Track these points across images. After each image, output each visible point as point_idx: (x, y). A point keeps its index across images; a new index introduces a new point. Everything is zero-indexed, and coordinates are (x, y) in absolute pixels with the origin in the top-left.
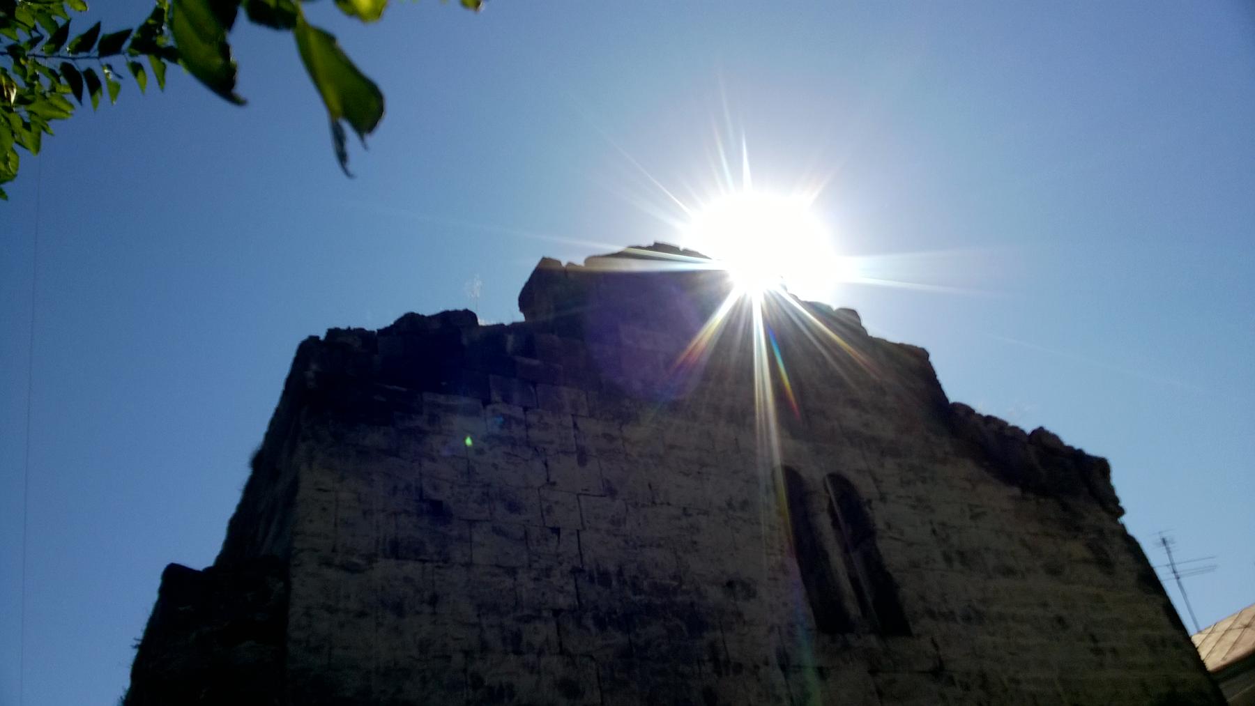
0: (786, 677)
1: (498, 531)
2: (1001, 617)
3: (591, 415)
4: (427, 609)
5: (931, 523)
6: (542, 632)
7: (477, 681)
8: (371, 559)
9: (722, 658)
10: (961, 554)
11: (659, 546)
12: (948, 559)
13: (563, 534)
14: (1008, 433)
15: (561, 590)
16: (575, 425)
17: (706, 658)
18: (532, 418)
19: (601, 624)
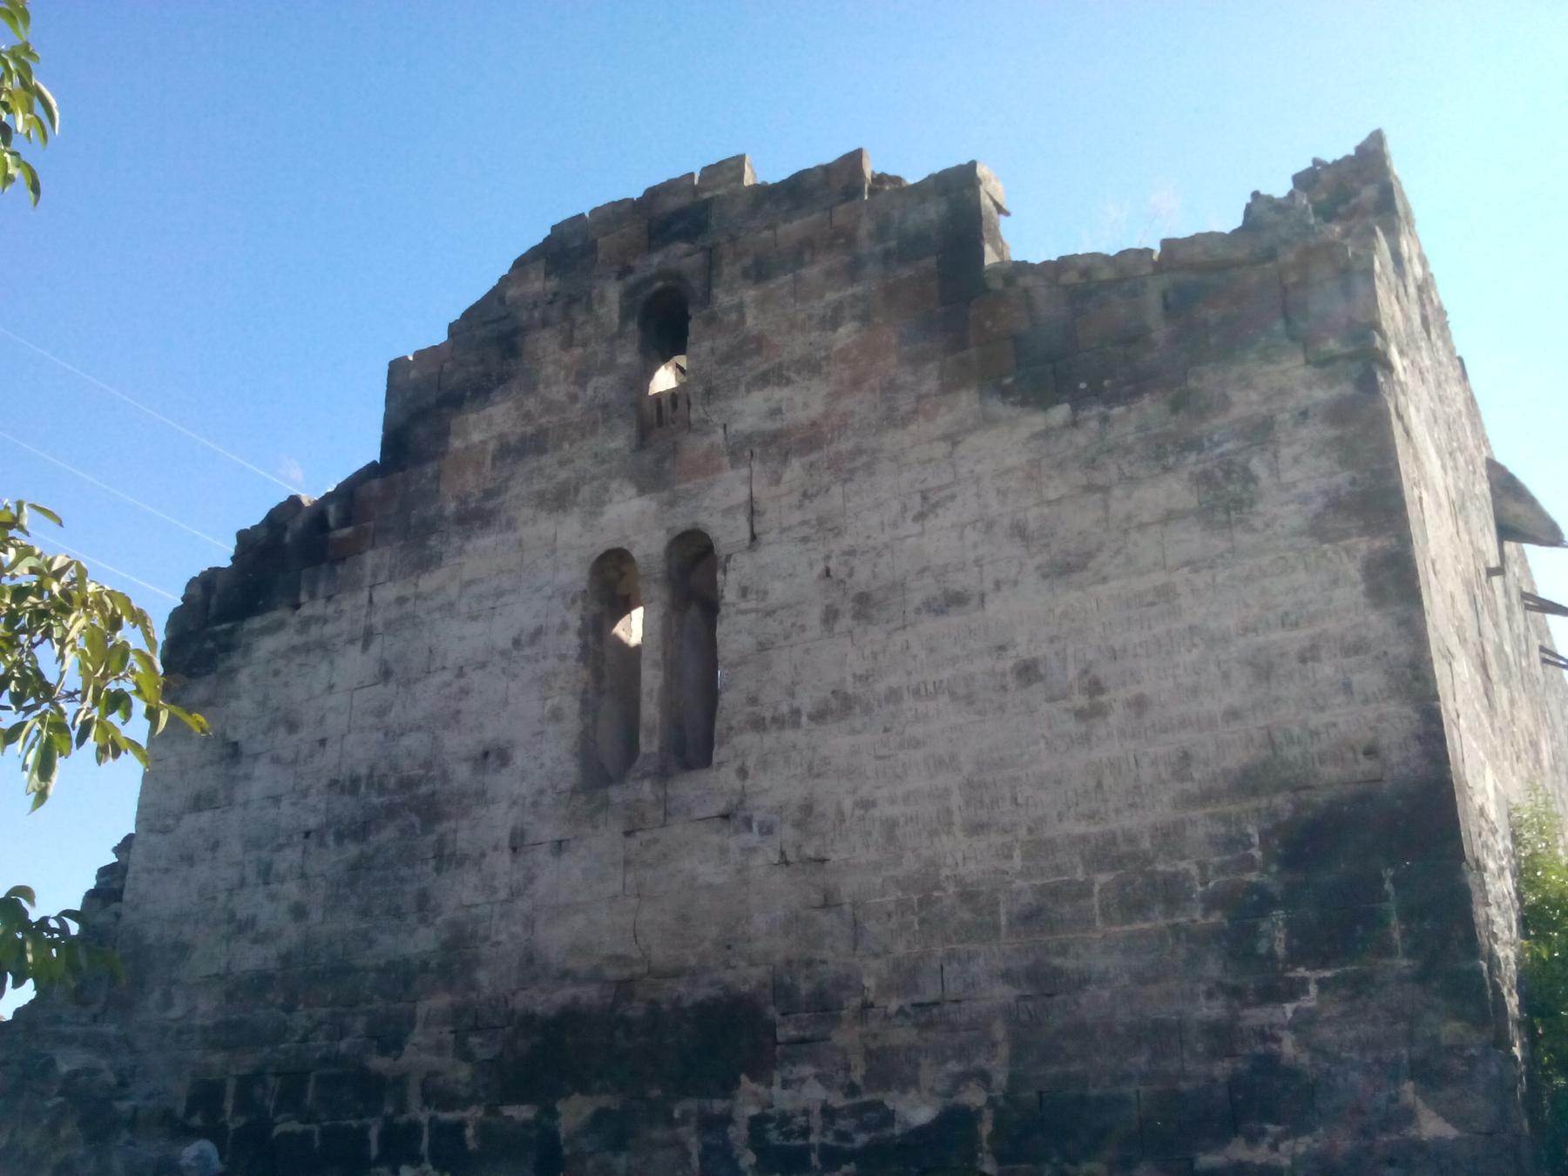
0: (513, 861)
1: (276, 760)
2: (893, 696)
3: (391, 578)
4: (209, 855)
5: (828, 557)
6: (290, 858)
7: (232, 917)
8: (178, 818)
9: (447, 852)
10: (863, 599)
11: (419, 728)
12: (831, 616)
13: (329, 743)
14: (1106, 274)
15: (314, 810)
16: (371, 601)
17: (431, 855)
18: (331, 609)
19: (340, 838)
